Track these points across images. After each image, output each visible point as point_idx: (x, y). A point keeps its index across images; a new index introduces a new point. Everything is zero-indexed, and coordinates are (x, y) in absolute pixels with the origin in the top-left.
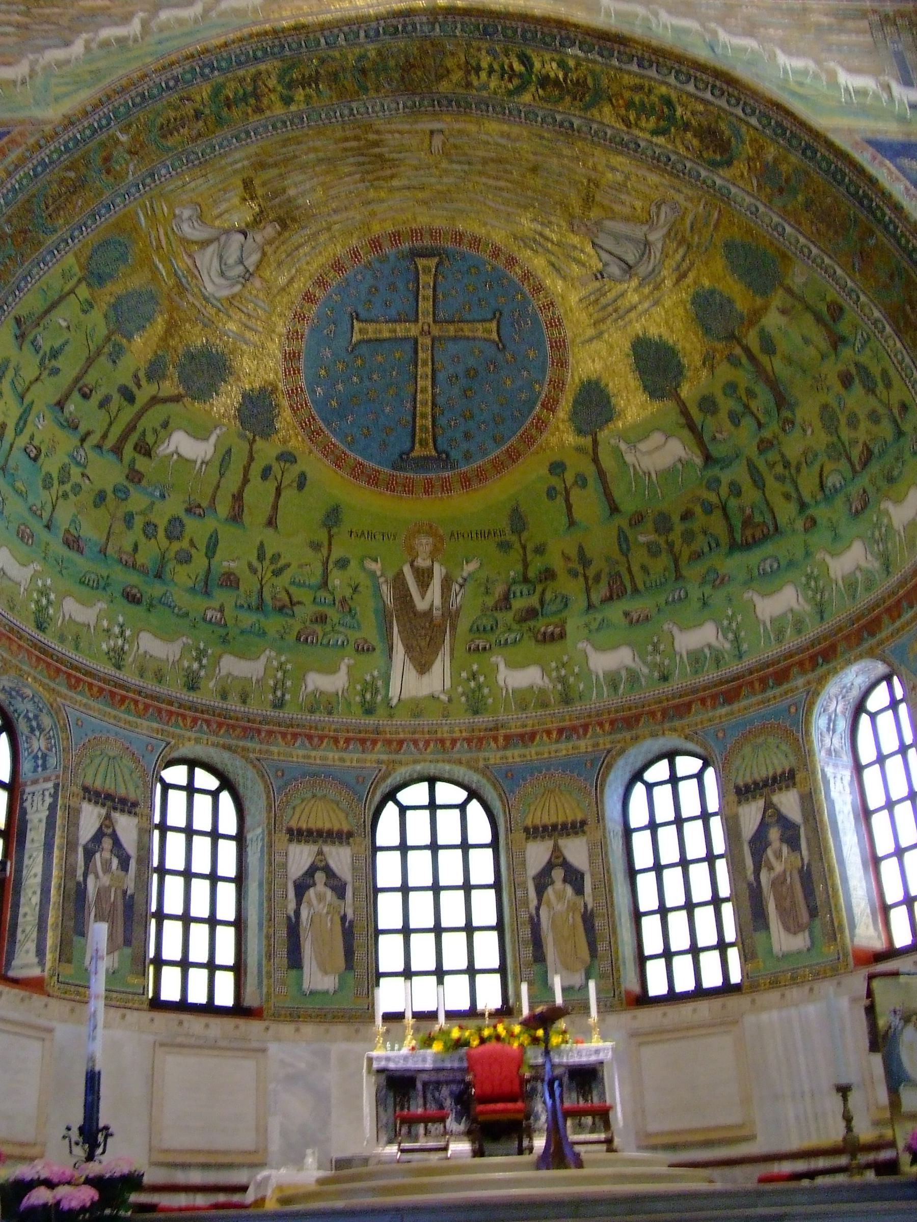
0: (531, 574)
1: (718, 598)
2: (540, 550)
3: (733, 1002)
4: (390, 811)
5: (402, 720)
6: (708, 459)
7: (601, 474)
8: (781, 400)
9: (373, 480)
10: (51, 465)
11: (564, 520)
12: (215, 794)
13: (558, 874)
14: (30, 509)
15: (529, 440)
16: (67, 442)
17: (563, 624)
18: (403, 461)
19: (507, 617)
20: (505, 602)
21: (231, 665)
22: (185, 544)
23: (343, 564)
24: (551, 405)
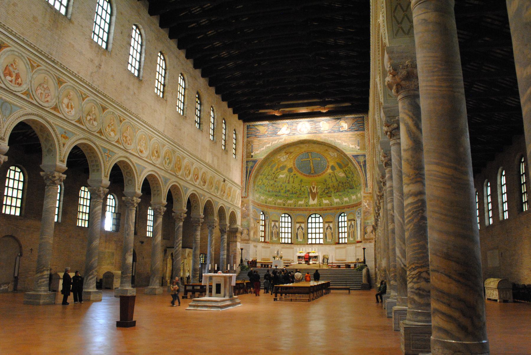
0: (327, 188)
1: (349, 194)
2: (328, 185)
3: (346, 245)
4: (310, 218)
5: (311, 207)
6: (347, 177)
7: (335, 176)
8: (353, 173)
9: (306, 176)
10: (266, 184)
11: (331, 181)
12: (288, 217)
13: (329, 228)
14: (264, 190)
15: (326, 171)
16: (267, 181)
17: (331, 195)
18: (310, 173)
19: (324, 193)
20: (324, 191)
21: (289, 202)
22: (282, 187)
23: (303, 187)
24: (328, 167)
